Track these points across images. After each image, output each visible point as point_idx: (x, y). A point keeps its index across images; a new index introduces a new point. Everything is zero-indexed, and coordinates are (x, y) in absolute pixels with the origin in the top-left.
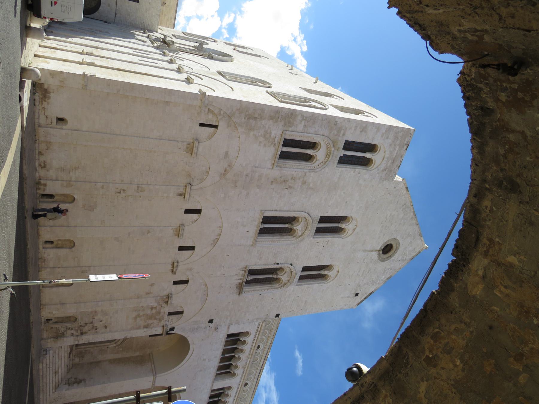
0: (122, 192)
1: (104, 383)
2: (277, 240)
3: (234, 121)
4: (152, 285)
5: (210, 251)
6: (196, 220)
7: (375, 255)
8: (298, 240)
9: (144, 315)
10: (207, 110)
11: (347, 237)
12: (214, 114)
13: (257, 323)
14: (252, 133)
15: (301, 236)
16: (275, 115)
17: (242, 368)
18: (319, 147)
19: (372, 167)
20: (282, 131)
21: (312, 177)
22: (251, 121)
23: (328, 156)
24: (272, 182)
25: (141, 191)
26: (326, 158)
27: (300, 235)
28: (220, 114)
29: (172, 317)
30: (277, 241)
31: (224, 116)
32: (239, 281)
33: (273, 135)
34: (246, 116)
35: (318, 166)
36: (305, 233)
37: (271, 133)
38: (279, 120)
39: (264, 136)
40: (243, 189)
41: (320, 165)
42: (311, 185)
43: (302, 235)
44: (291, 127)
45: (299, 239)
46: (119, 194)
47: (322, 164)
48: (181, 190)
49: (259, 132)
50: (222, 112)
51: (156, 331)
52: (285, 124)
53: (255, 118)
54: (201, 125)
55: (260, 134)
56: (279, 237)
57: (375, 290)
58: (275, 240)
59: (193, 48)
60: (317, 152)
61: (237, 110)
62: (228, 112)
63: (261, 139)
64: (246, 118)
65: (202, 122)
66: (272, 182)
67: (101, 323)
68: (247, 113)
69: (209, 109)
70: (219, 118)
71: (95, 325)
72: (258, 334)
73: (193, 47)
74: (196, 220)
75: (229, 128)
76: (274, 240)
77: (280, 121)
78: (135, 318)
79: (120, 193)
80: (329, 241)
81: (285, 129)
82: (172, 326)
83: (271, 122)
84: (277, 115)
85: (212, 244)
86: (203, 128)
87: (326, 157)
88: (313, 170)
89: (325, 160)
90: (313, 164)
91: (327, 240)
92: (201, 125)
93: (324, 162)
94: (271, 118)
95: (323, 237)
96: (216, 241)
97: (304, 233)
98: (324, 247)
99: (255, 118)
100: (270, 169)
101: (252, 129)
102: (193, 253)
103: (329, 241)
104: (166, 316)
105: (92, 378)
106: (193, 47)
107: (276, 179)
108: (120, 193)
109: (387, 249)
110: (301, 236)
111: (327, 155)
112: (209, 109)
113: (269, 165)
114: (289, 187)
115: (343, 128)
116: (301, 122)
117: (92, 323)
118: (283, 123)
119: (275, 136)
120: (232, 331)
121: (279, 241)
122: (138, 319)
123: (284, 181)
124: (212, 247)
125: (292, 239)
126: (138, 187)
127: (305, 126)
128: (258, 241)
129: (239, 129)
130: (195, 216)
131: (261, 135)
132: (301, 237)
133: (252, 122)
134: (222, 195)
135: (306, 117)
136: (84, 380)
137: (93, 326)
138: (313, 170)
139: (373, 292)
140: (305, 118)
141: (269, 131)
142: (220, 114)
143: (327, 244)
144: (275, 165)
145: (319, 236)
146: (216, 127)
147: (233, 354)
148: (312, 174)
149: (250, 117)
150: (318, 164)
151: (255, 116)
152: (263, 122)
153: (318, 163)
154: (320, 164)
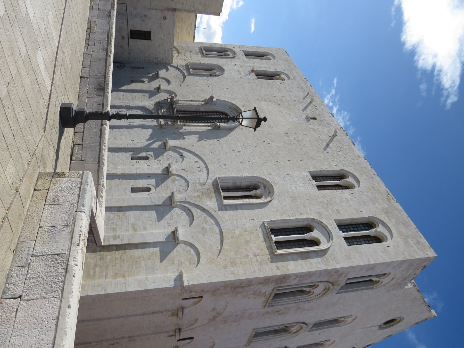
0: (115, 344)
7: (377, 328)
10: (189, 291)
11: (345, 325)
14: (239, 295)
19: (378, 285)
20: (272, 288)
22: (238, 289)
30: (271, 339)
35: (314, 297)
37: (260, 291)
43: (296, 332)
44: (283, 284)
45: (294, 335)
48: (171, 334)
50: (205, 290)
52: (277, 284)
53: (243, 287)
54: (183, 299)
57: (373, 344)
58: (269, 338)
59: (203, 103)
60: (314, 289)
61: (222, 286)
66: (264, 315)
68: (233, 286)
73: (202, 101)
76: (267, 338)
77: (271, 283)
80: (325, 330)
81: (277, 286)
87: (325, 291)
89: (323, 293)
90: (310, 295)
92: (183, 299)
93: (321, 294)
95: (320, 329)
98: (319, 334)
99: (243, 287)
100: (261, 308)
101: (241, 293)
106: (202, 101)
109: (390, 322)
111: (325, 289)
114: (282, 313)
118: (274, 283)
119: (265, 292)
121: (273, 338)
123: (277, 311)
125: (287, 335)
128: (253, 342)
132: (295, 334)
133: (240, 290)
139: (371, 345)
140: (300, 276)
141: (258, 291)
144: (266, 306)
146: (202, 297)
149: (235, 288)
151: (242, 286)
152: (252, 287)
153: (314, 295)
154: (317, 295)
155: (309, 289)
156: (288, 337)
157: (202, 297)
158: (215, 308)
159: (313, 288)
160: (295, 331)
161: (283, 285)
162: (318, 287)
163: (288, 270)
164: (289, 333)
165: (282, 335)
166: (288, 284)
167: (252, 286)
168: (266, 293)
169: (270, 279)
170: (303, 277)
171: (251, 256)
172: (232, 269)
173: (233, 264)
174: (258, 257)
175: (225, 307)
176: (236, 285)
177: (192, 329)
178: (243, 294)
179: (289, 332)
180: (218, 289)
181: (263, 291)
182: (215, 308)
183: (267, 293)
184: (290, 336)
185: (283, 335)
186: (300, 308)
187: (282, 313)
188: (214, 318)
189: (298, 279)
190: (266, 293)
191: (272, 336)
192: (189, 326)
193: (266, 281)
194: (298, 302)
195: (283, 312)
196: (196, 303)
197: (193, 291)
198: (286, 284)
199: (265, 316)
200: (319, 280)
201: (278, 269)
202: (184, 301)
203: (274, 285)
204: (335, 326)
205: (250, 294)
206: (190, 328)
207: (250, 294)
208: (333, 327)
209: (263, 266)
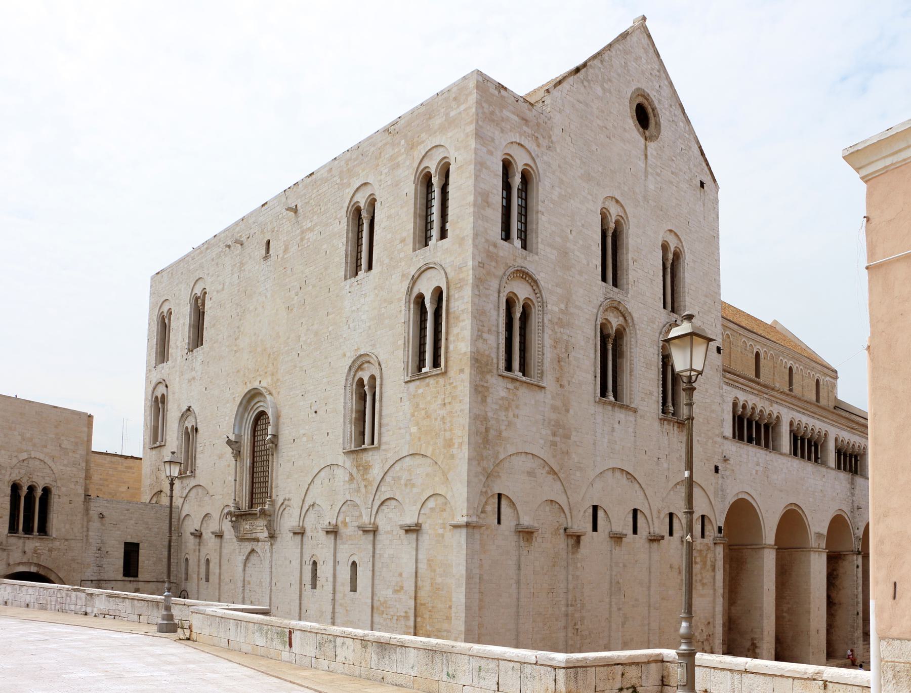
0: (577, 627)
1: (761, 616)
2: (628, 364)
3: (492, 467)
4: (671, 567)
5: (640, 485)
6: (605, 512)
8: (631, 324)
9: (701, 573)
10: (483, 515)
12: (486, 503)
13: (725, 387)
14: (504, 434)
15: (625, 318)
16: (480, 392)
17: (772, 406)
18: (511, 295)
21: (553, 307)
22: (490, 437)
23: (524, 277)
24: (561, 386)
25: (576, 601)
26: (527, 279)
27: (623, 321)
28: (486, 492)
29: (707, 533)
30: (630, 365)
31: (488, 486)
32: (675, 428)
33: (503, 394)
34: (485, 447)
35: (538, 295)
36: (622, 311)
37: (502, 398)
38: (485, 385)
39: (507, 409)
40: (569, 438)
41: (536, 291)
42: (563, 306)
44: (492, 359)
45: (630, 321)
46: (579, 631)
47: (535, 287)
49: (503, 420)
50: (484, 490)
51: (719, 554)
52: (490, 371)
53: (487, 430)
54: (499, 522)
55: (504, 418)
56: (625, 360)
60: (518, 299)
61: (479, 464)
62: (484, 480)
63: (511, 414)
64: (488, 446)
65: (496, 521)
66: (561, 386)
67: (704, 631)
68: (482, 446)
69: (482, 512)
70: (490, 494)
71: (705, 638)
72: (737, 384)
74: (605, 512)
75: (500, 474)
78: (703, 585)
79: (577, 629)
80: (632, 258)
81: (495, 371)
82: (716, 529)
83: (489, 400)
84: (480, 389)
85: (632, 482)
86: (502, 517)
88: (545, 305)
89: (530, 281)
91: (631, 262)
92: (499, 522)
93: (532, 284)
94: (484, 400)
96: (629, 476)
97: (621, 313)
99: (487, 430)
101: (500, 433)
102: (641, 511)
103: (632, 258)
104: (705, 540)
105: (752, 630)
107: (558, 380)
108: (577, 629)
110: (625, 318)
112: (482, 512)
113: (540, 396)
115: (487, 247)
116: (484, 340)
117: (703, 642)
118: (488, 377)
119: (505, 390)
120: (728, 431)
122: (705, 581)
123: (559, 362)
124: (635, 481)
125: (628, 335)
126: (572, 605)
127: (489, 331)
129: (502, 457)
130: (601, 514)
131: (505, 415)
133: (492, 433)
134: (578, 474)
135: (478, 331)
136: (752, 639)
137: (707, 640)
138: (543, 304)
140: (480, 333)
141: (501, 402)
142: (486, 492)
143: (636, 262)
145: (622, 281)
146: (500, 495)
147: (754, 423)
148: (549, 307)
149: (486, 441)
150: (534, 295)
151: (484, 431)
152: (490, 414)
155: (517, 308)
156: (632, 332)
157: (500, 495)
158: (528, 472)
159: (516, 301)
160: (621, 318)
161: (495, 361)
162: (516, 292)
163: (465, 353)
164: (625, 329)
165: (626, 346)
166: (495, 350)
167: (487, 415)
168: (507, 388)
169: (476, 386)
170: (483, 326)
171: (443, 412)
172: (456, 446)
173: (449, 444)
174: (446, 401)
175: (531, 456)
176: (480, 441)
177: (570, 509)
178: (503, 428)
179: (622, 329)
180: (484, 469)
181: (503, 394)
182: (528, 472)
183: (510, 386)
184: (631, 328)
185: (626, 341)
186: (559, 319)
187: (566, 351)
188: (552, 472)
189: (485, 336)
190: (507, 388)
191: (627, 362)
192: (564, 512)
193: (480, 391)
194: (543, 326)
195: (563, 350)
196: (512, 504)
197: (484, 507)
198: (494, 355)
199: (566, 383)
200: (496, 295)
201: (462, 371)
202: (502, 522)
203: (492, 376)
204: (627, 238)
205: (507, 416)
206: (567, 511)
207: (507, 416)
208: (627, 244)
209: (456, 396)
